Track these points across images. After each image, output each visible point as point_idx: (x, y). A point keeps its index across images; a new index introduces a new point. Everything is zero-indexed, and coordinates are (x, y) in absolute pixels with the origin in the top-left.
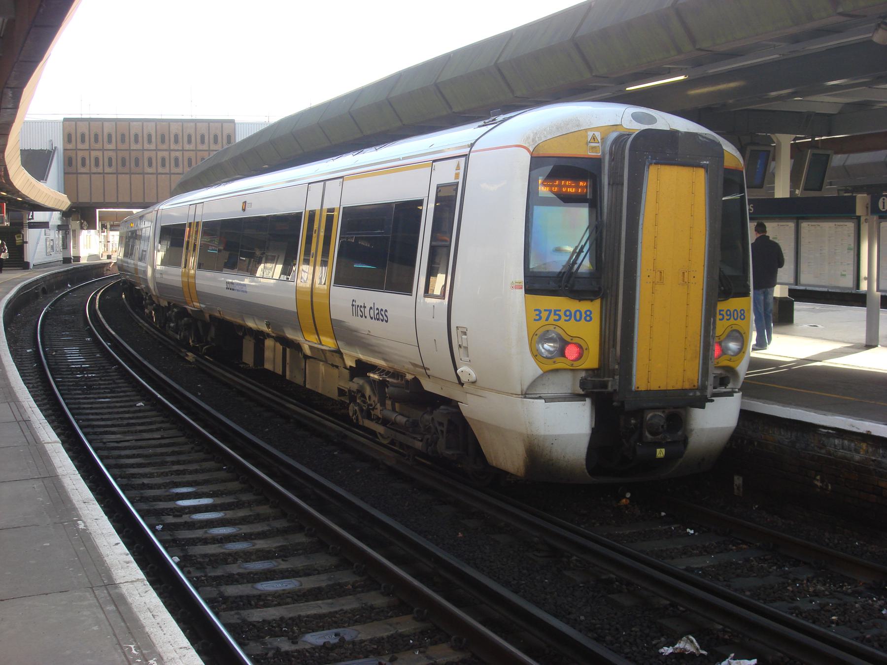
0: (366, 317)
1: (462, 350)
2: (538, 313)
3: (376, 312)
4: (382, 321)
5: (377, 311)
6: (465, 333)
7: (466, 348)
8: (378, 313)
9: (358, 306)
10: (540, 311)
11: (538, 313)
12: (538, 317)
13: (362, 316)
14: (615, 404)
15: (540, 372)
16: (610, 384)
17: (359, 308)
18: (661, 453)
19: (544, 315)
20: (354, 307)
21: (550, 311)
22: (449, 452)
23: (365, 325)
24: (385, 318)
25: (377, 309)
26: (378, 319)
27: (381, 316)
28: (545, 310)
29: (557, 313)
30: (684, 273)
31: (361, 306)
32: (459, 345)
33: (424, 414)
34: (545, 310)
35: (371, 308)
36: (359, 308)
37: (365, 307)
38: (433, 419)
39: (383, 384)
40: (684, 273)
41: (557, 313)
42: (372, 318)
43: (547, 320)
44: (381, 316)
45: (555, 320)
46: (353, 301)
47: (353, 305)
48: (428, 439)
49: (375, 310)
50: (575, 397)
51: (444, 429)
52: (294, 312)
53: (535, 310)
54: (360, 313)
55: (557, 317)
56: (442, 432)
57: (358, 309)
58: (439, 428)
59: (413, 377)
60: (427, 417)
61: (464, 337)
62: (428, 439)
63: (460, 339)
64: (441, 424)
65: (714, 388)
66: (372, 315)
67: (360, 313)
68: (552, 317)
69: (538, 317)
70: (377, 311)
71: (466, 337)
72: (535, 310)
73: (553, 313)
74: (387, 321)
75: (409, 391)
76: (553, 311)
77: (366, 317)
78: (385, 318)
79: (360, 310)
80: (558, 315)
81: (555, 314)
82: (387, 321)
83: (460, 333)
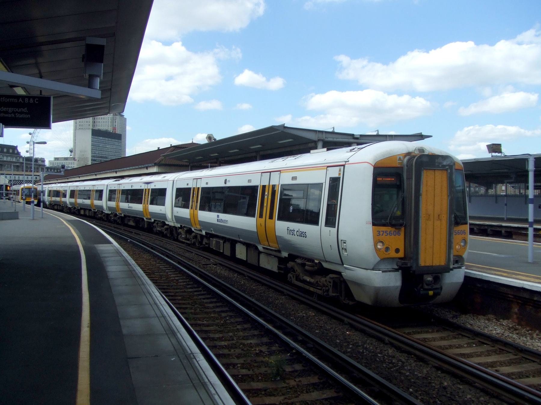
0: (295, 235)
1: (343, 250)
2: (379, 232)
3: (300, 233)
4: (304, 237)
5: (301, 233)
6: (345, 243)
7: (346, 249)
8: (301, 234)
9: (290, 230)
10: (379, 232)
11: (379, 232)
12: (378, 234)
13: (293, 235)
14: (411, 272)
15: (380, 259)
16: (409, 264)
17: (291, 231)
18: (431, 293)
19: (381, 233)
20: (288, 231)
21: (383, 231)
22: (334, 295)
23: (295, 239)
24: (305, 236)
25: (301, 232)
26: (301, 236)
27: (303, 234)
28: (381, 231)
29: (387, 232)
30: (439, 215)
31: (292, 230)
32: (343, 248)
33: (321, 278)
34: (381, 231)
35: (297, 231)
36: (291, 231)
37: (294, 231)
38: (326, 281)
39: (303, 265)
40: (439, 215)
41: (387, 232)
42: (298, 236)
43: (382, 235)
44: (303, 235)
45: (386, 235)
46: (288, 227)
47: (288, 230)
48: (324, 289)
49: (300, 232)
50: (396, 270)
51: (331, 284)
52: (256, 232)
53: (378, 231)
54: (291, 233)
55: (386, 234)
56: (330, 286)
57: (291, 232)
58: (329, 284)
59: (319, 261)
60: (324, 279)
61: (345, 244)
62: (324, 289)
63: (342, 245)
64: (330, 282)
65: (453, 265)
66: (298, 234)
67: (291, 233)
68: (385, 234)
69: (378, 234)
70: (301, 233)
71: (345, 244)
72: (378, 231)
73: (384, 233)
74: (306, 237)
75: (317, 268)
76: (385, 232)
77: (295, 235)
78: (305, 236)
79: (293, 233)
80: (387, 233)
81: (386, 233)
82: (306, 237)
83: (342, 243)
